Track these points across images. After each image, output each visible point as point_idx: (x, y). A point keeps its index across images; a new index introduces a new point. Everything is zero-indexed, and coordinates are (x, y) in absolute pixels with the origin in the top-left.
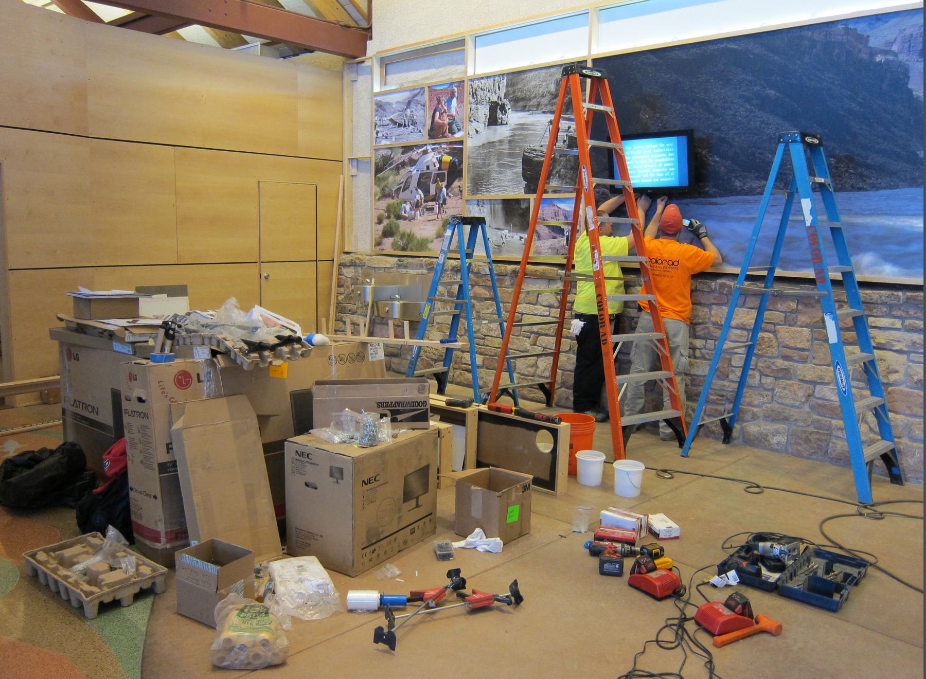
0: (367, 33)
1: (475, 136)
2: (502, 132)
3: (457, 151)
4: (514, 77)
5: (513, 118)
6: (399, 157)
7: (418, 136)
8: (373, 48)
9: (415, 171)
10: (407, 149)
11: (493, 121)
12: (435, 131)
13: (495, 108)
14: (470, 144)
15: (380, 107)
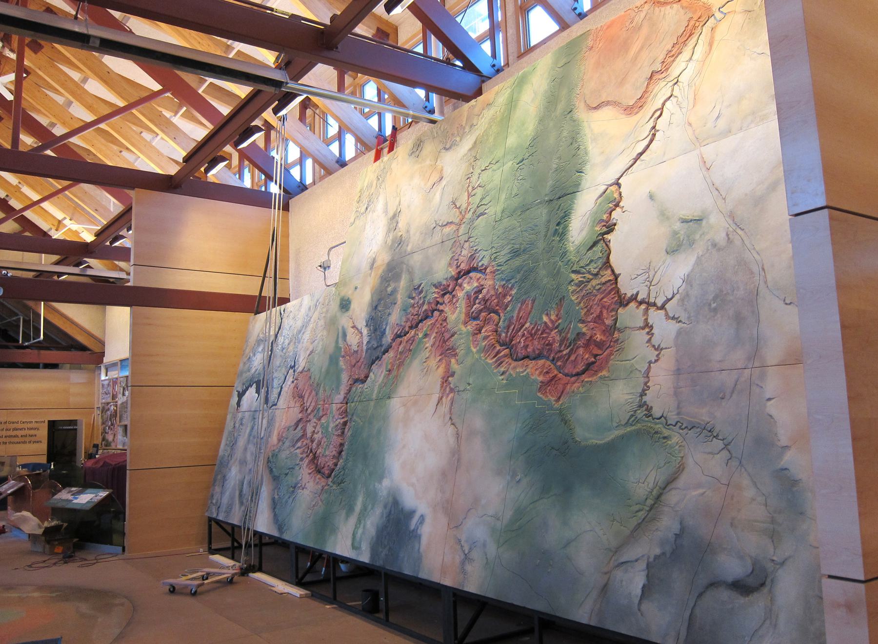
0: (103, 354)
1: (121, 400)
3: (116, 406)
6: (106, 408)
7: (109, 400)
8: (106, 360)
9: (109, 413)
10: (108, 403)
13: (124, 389)
14: (119, 403)
15: (103, 385)
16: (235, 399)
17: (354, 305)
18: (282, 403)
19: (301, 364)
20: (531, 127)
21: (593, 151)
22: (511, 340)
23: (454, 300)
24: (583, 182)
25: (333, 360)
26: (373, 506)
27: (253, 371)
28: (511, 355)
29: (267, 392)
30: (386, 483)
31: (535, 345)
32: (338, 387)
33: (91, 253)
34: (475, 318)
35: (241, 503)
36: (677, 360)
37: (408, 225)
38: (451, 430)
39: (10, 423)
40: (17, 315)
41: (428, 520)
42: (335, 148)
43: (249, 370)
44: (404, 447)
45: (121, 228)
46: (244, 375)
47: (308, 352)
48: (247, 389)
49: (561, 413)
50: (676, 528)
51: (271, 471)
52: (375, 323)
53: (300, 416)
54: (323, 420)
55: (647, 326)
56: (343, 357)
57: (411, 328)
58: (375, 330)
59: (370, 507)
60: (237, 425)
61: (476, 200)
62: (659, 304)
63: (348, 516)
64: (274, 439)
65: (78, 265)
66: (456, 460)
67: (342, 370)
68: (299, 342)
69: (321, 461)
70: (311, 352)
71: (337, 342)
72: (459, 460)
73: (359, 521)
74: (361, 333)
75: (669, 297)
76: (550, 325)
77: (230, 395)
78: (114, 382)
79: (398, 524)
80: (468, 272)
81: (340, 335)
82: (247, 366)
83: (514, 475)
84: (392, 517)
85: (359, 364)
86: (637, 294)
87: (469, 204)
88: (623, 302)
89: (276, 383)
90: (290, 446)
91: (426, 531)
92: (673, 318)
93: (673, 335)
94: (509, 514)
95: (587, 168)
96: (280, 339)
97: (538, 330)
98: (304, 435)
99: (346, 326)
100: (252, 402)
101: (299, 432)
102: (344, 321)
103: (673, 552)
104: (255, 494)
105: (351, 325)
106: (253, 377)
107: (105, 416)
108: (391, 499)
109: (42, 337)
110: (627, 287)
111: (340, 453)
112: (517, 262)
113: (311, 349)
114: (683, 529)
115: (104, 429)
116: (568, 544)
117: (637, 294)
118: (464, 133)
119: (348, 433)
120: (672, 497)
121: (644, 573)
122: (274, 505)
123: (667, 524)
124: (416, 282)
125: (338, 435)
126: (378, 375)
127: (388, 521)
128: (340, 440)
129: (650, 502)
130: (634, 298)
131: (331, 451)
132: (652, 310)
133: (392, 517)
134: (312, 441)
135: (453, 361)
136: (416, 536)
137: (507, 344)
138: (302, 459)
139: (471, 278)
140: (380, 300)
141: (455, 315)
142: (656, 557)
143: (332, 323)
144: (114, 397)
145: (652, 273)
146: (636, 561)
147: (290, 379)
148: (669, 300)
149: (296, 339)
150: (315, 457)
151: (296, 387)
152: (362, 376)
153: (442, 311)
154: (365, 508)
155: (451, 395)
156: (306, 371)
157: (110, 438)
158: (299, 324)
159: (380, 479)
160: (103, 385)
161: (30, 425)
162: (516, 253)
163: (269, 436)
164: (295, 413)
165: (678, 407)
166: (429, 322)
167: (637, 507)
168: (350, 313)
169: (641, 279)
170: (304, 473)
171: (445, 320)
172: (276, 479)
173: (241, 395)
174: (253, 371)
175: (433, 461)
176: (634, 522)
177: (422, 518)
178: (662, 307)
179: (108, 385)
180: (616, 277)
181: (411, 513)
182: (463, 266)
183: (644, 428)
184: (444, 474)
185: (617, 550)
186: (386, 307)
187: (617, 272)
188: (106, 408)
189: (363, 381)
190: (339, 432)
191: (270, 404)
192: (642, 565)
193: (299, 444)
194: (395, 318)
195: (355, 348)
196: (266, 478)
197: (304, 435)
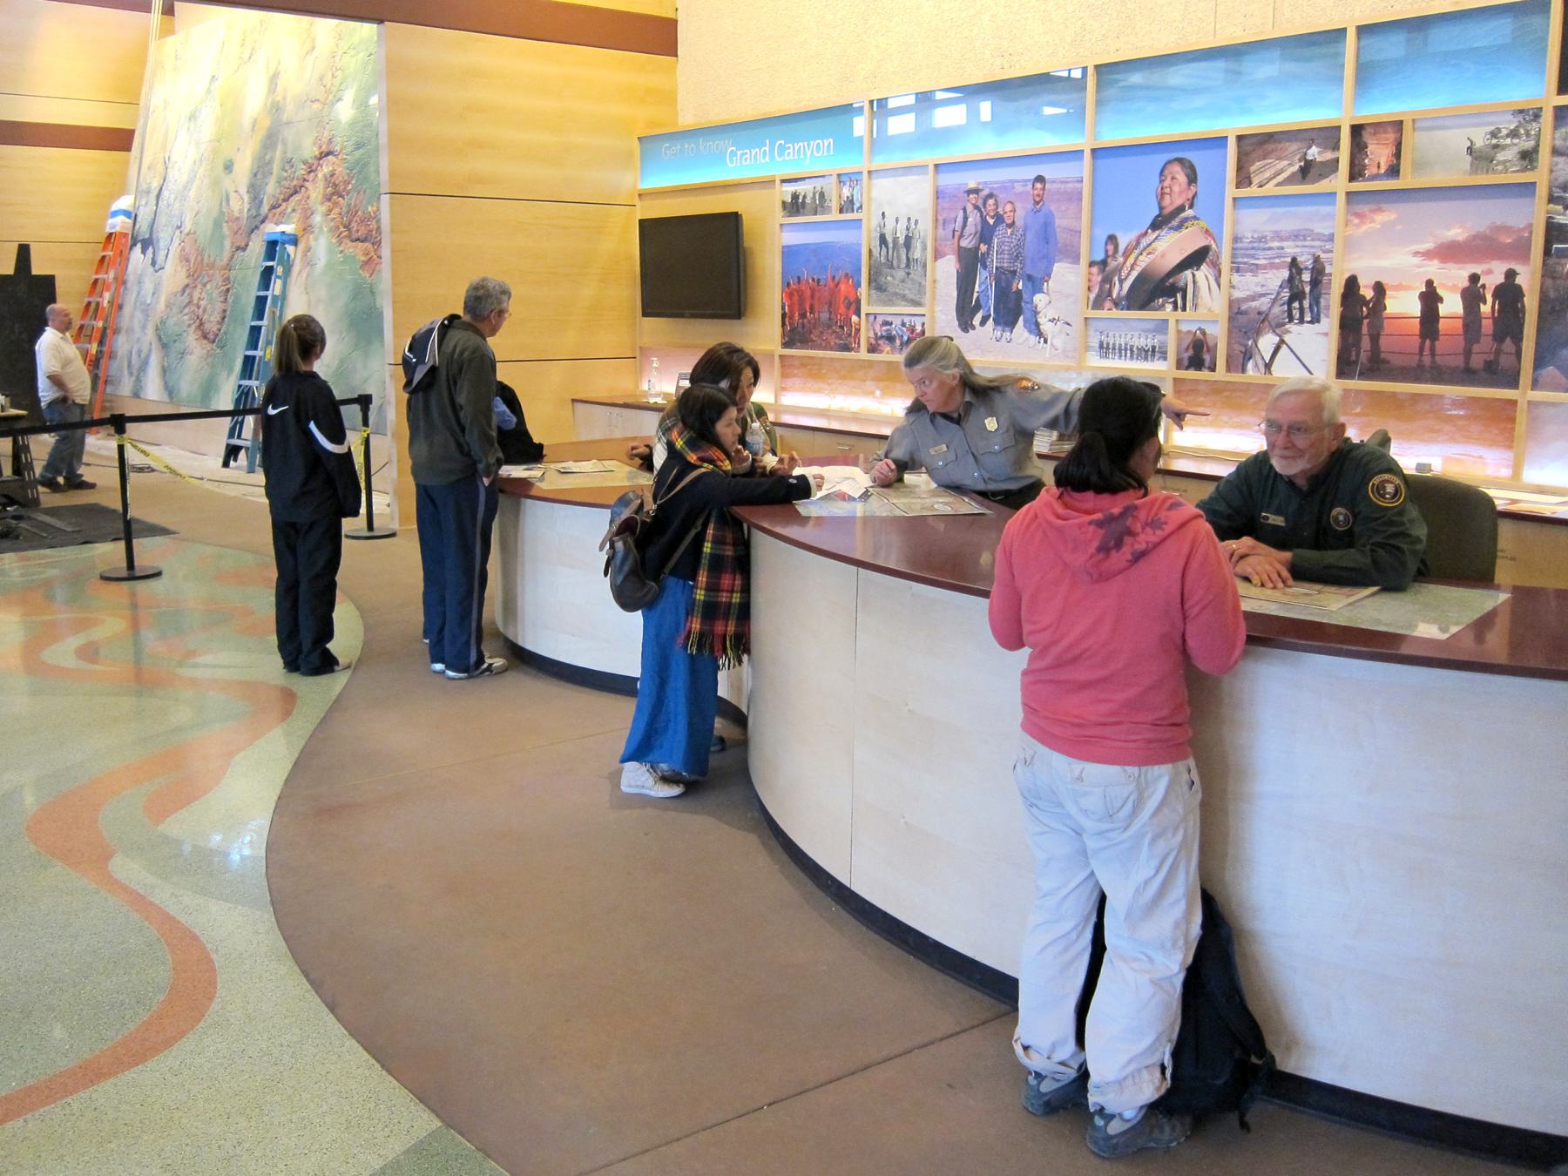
17: (236, 167)
18: (169, 267)
19: (188, 227)
25: (217, 224)
28: (349, 237)
31: (363, 232)
32: (222, 251)
35: (131, 374)
51: (160, 339)
52: (255, 191)
57: (284, 200)
61: (337, 82)
64: (161, 306)
69: (207, 326)
80: (328, 154)
89: (162, 244)
96: (165, 193)
102: (227, 183)
104: (145, 364)
112: (358, 154)
119: (230, 300)
122: (164, 371)
124: (289, 155)
128: (222, 306)
131: (216, 317)
137: (347, 227)
141: (316, 191)
143: (215, 183)
147: (176, 241)
149: (182, 196)
150: (201, 324)
151: (183, 250)
158: (185, 178)
162: (359, 146)
164: (182, 279)
166: (297, 197)
170: (191, 339)
172: (164, 346)
182: (324, 148)
186: (265, 176)
189: (244, 249)
194: (271, 189)
196: (155, 346)
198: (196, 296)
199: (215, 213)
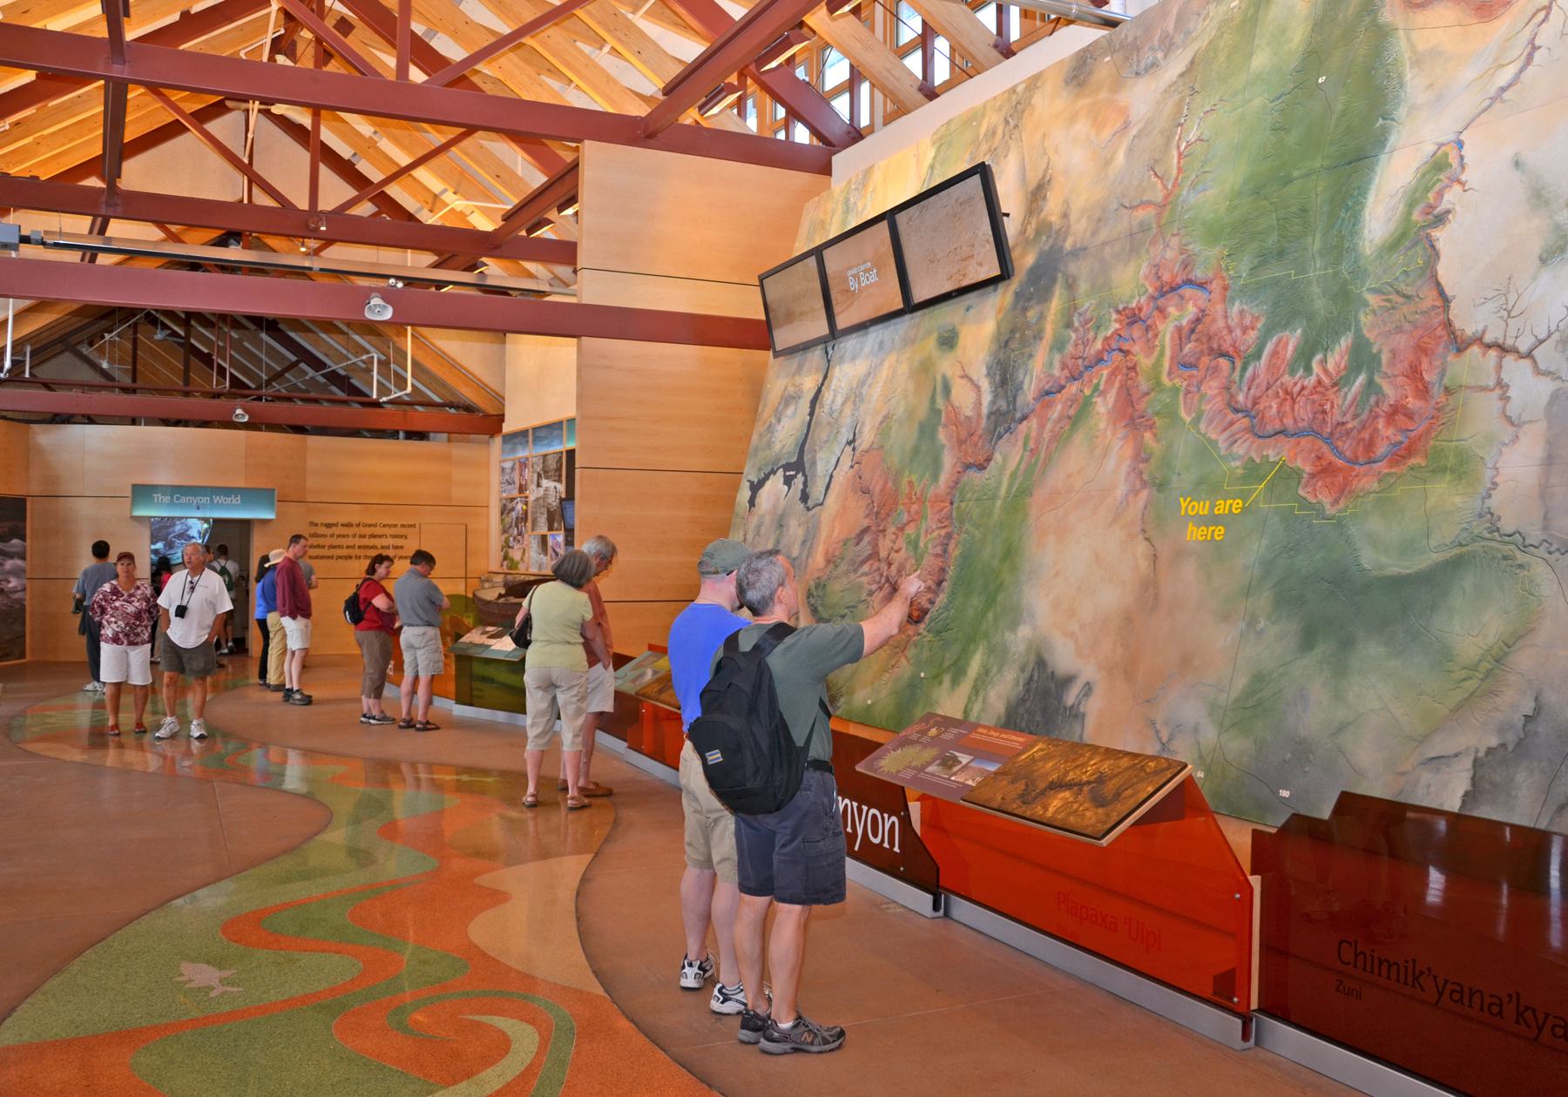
0: (501, 418)
1: (533, 494)
2: (541, 491)
4: (545, 456)
5: (545, 483)
6: (510, 506)
7: (515, 493)
8: (507, 427)
9: (514, 514)
10: (512, 500)
11: (539, 485)
12: (522, 489)
13: (539, 475)
14: (532, 498)
16: (744, 494)
19: (867, 438)
20: (1298, 36)
21: (1414, 84)
22: (1255, 403)
23: (1150, 334)
24: (1393, 139)
25: (927, 430)
26: (1001, 667)
27: (777, 447)
28: (1250, 430)
29: (805, 484)
30: (1024, 631)
32: (935, 477)
33: (496, 247)
34: (1185, 366)
36: (1548, 442)
37: (1067, 203)
38: (1142, 548)
39: (366, 525)
40: (368, 352)
41: (1098, 691)
42: (914, 62)
43: (769, 445)
44: (1057, 574)
45: (547, 208)
46: (761, 455)
47: (879, 418)
48: (767, 477)
49: (1340, 524)
50: (1528, 707)
53: (866, 523)
54: (910, 530)
55: (1500, 384)
56: (945, 426)
58: (1004, 382)
59: (995, 669)
60: (750, 537)
62: (1523, 348)
63: (955, 682)
64: (819, 559)
65: (472, 268)
66: (1149, 593)
67: (943, 446)
68: (862, 401)
70: (886, 417)
71: (933, 400)
72: (1156, 596)
73: (976, 690)
74: (978, 388)
75: (1542, 336)
76: (1326, 381)
77: (736, 488)
78: (523, 465)
79: (1043, 700)
81: (939, 389)
82: (765, 440)
83: (1252, 622)
84: (1034, 685)
85: (975, 438)
86: (1484, 332)
87: (1180, 170)
88: (1460, 345)
90: (846, 573)
91: (1093, 707)
92: (1548, 373)
93: (1544, 399)
94: (1241, 682)
95: (1401, 112)
96: (827, 396)
97: (1303, 388)
98: (874, 555)
99: (949, 374)
100: (778, 500)
101: (865, 547)
102: (946, 366)
103: (1519, 744)
105: (960, 373)
106: (778, 459)
107: (508, 520)
108: (1032, 658)
109: (409, 389)
110: (1468, 320)
111: (939, 583)
113: (884, 413)
114: (1538, 709)
115: (507, 541)
116: (1341, 728)
117: (1484, 332)
118: (1171, 45)
120: (1524, 660)
121: (1469, 774)
123: (1514, 703)
125: (937, 555)
126: (1009, 456)
127: (1028, 691)
128: (938, 562)
129: (1485, 666)
130: (1478, 340)
132: (1509, 359)
133: (1034, 685)
134: (890, 565)
135: (1148, 435)
136: (1076, 716)
138: (871, 594)
139: (1182, 297)
140: (1013, 331)
142: (1490, 751)
144: (522, 489)
145: (1512, 297)
146: (1456, 755)
148: (1541, 342)
152: (981, 459)
153: (1126, 353)
154: (985, 673)
155: (1145, 494)
156: (878, 448)
157: (516, 554)
159: (1013, 627)
160: (503, 470)
161: (393, 531)
163: (809, 554)
164: (858, 516)
165: (1545, 517)
167: (1464, 673)
168: (959, 351)
169: (1491, 306)
171: (1133, 368)
173: (756, 488)
174: (777, 447)
175: (1111, 597)
176: (1458, 696)
177: (1088, 689)
178: (1529, 355)
179: (513, 469)
180: (1445, 300)
181: (1069, 680)
183: (1488, 553)
184: (1128, 619)
185: (1423, 740)
186: (1024, 342)
187: (1449, 292)
188: (510, 506)
189: (981, 467)
190: (939, 550)
191: (810, 503)
192: (1467, 763)
193: (866, 568)
195: (968, 411)
197: (874, 555)
198: (884, 546)
199: (922, 412)
